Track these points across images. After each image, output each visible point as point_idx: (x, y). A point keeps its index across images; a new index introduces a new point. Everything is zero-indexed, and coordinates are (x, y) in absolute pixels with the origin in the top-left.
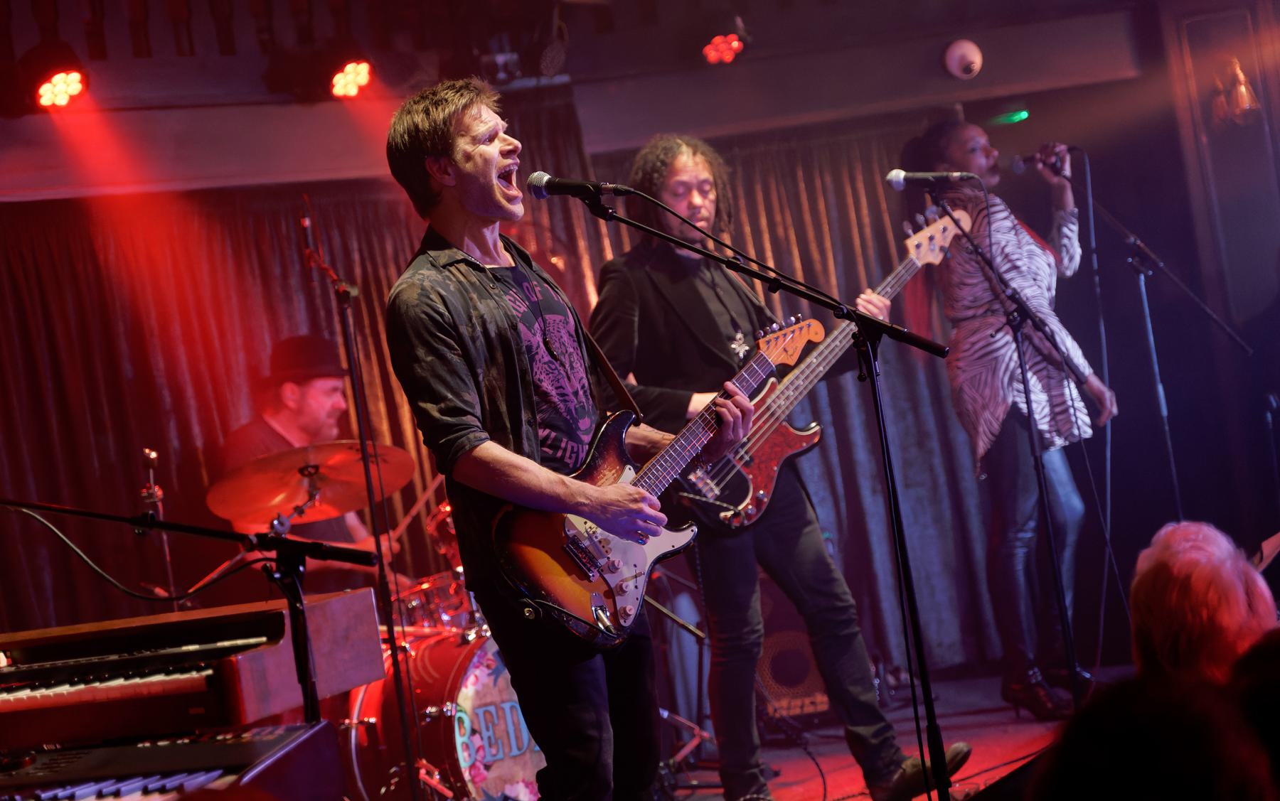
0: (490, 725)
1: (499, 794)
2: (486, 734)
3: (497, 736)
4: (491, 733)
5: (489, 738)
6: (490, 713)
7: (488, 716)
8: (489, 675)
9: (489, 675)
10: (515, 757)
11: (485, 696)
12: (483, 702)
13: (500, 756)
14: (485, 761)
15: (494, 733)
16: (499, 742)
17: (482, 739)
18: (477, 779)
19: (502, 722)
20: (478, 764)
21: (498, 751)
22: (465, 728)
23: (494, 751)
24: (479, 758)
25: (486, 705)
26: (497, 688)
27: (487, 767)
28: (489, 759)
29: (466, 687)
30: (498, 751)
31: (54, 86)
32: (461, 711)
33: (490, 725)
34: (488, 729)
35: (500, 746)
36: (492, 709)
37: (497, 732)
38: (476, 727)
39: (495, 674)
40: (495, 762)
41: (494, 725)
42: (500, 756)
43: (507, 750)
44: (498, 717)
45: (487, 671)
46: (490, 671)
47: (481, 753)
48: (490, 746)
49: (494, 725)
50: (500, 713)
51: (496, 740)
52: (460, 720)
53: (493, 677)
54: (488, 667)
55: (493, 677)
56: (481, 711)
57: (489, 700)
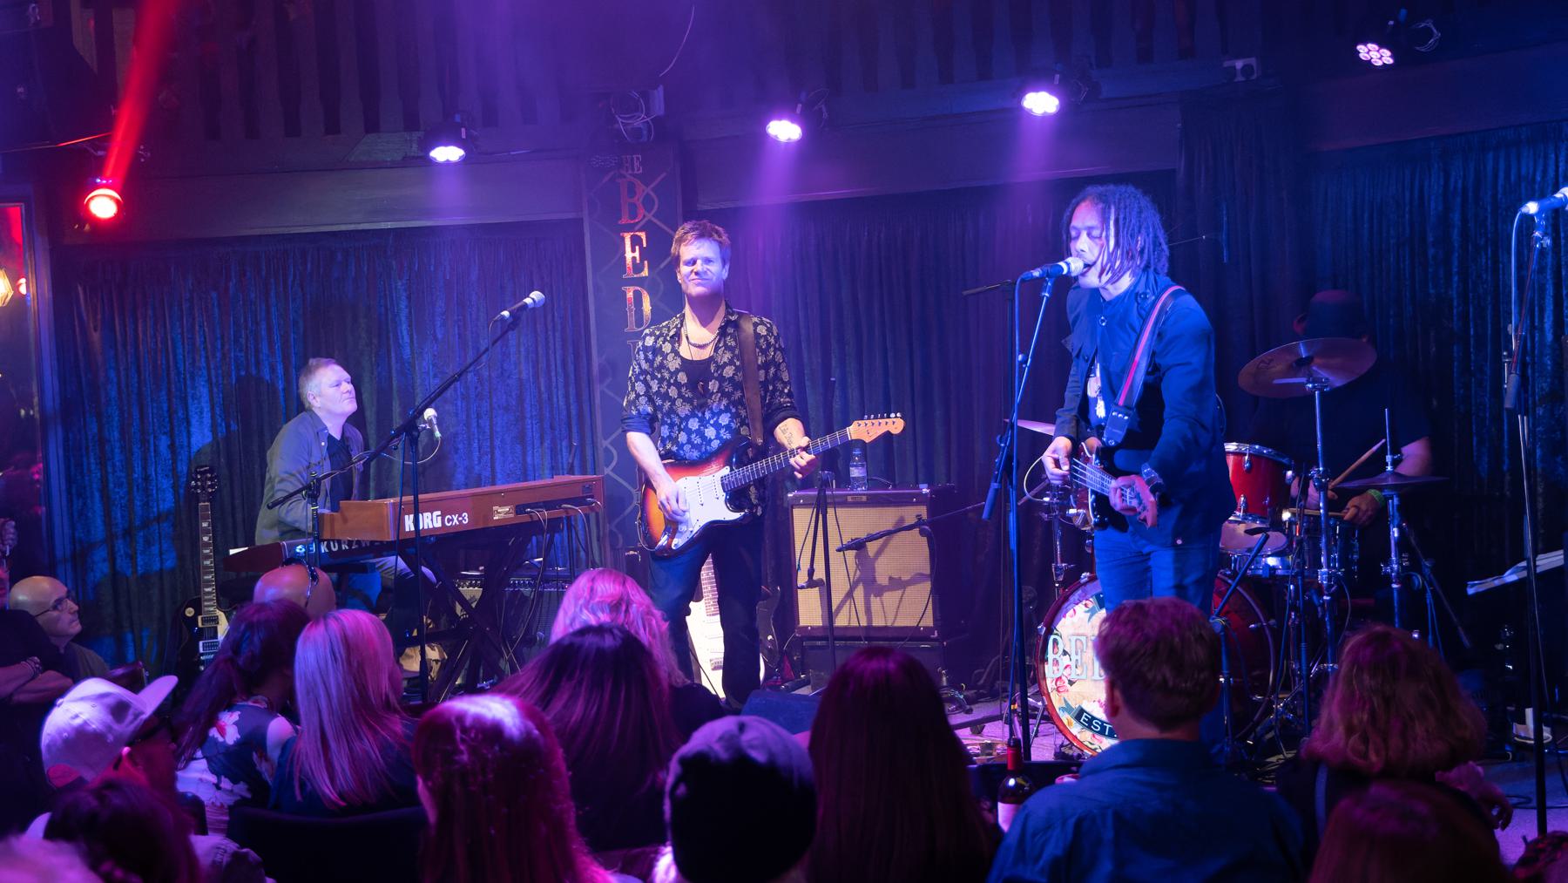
1: (1077, 706)
2: (1074, 657)
3: (1084, 660)
4: (1078, 657)
5: (1077, 660)
6: (1082, 643)
7: (1079, 643)
8: (1086, 612)
9: (1086, 612)
10: (1095, 681)
12: (1077, 632)
13: (1084, 677)
15: (1081, 659)
18: (1061, 690)
20: (1064, 678)
23: (1079, 671)
24: (1066, 674)
25: (1078, 635)
27: (1071, 683)
28: (1069, 678)
32: (1056, 634)
34: (1077, 654)
35: (1085, 669)
36: (1083, 639)
39: (1092, 612)
41: (1082, 651)
42: (1084, 677)
43: (1090, 673)
44: (1087, 646)
45: (1083, 607)
46: (1087, 609)
47: (1068, 669)
49: (1082, 651)
51: (1082, 665)
52: (1055, 642)
53: (1089, 614)
54: (1086, 605)
55: (1089, 614)
57: (1081, 631)
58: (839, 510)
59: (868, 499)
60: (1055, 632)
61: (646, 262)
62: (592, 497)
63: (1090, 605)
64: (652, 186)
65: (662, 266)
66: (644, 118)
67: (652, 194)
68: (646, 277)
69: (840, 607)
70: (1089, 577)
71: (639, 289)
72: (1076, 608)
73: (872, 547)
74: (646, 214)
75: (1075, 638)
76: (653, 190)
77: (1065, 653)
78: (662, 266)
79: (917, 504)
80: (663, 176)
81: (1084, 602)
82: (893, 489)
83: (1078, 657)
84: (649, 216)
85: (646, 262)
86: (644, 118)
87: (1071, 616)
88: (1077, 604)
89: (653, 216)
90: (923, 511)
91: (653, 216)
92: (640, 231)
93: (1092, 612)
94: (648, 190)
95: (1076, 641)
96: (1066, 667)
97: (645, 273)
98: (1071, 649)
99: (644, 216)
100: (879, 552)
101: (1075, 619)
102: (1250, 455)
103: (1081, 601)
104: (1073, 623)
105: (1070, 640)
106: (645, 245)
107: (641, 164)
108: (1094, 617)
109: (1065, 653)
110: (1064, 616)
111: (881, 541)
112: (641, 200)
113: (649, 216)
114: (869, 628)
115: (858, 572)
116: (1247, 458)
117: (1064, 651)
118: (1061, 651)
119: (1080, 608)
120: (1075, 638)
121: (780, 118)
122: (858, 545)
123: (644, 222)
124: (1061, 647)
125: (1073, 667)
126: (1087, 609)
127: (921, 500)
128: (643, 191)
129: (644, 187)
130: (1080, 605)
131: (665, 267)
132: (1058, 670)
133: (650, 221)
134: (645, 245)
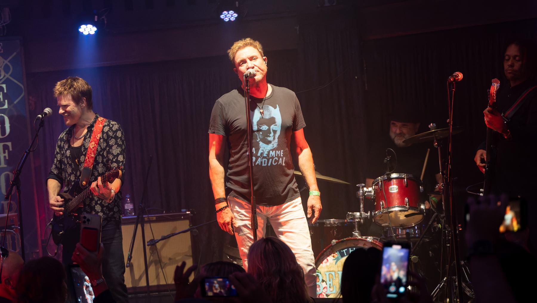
0: (331, 279)
2: (328, 283)
3: (334, 284)
4: (331, 282)
5: (330, 284)
6: (332, 274)
7: (331, 276)
11: (330, 268)
12: (329, 270)
14: (326, 293)
16: (335, 286)
17: (326, 284)
19: (337, 279)
20: (323, 294)
21: (333, 290)
22: (319, 279)
23: (331, 289)
24: (324, 291)
25: (330, 271)
26: (336, 265)
28: (328, 293)
29: (322, 263)
30: (333, 290)
31: (229, 18)
32: (318, 272)
33: (331, 279)
34: (330, 281)
36: (333, 273)
37: (334, 282)
38: (324, 279)
39: (337, 260)
40: (331, 294)
41: (333, 279)
44: (335, 277)
45: (332, 257)
46: (334, 258)
47: (325, 289)
48: (330, 287)
49: (333, 279)
50: (337, 275)
53: (335, 261)
54: (333, 256)
56: (327, 274)
57: (332, 269)
58: (152, 224)
59: (156, 218)
60: (317, 271)
61: (6, 101)
62: (14, 225)
63: (336, 256)
64: (10, 58)
65: (15, 102)
66: (2, 24)
67: (9, 64)
68: (5, 109)
69: (140, 278)
70: (336, 242)
71: (3, 115)
72: (328, 258)
73: (159, 245)
74: (6, 74)
75: (328, 273)
76: (9, 62)
77: (323, 281)
78: (15, 102)
79: (184, 219)
80: (15, 53)
81: (332, 255)
82: (165, 214)
83: (331, 282)
84: (8, 76)
85: (6, 101)
86: (2, 24)
87: (326, 263)
88: (329, 256)
89: (10, 75)
90: (187, 222)
91: (10, 75)
92: (3, 83)
93: (337, 260)
94: (6, 62)
95: (329, 274)
96: (324, 288)
97: (6, 106)
98: (327, 279)
99: (4, 76)
100: (163, 246)
101: (328, 264)
102: (406, 178)
103: (330, 255)
104: (327, 266)
105: (325, 274)
106: (5, 91)
107: (2, 48)
108: (338, 262)
109: (323, 281)
110: (322, 262)
111: (164, 240)
112: (2, 67)
113: (8, 76)
114: (159, 286)
115: (152, 258)
116: (405, 180)
117: (323, 280)
118: (321, 280)
119: (330, 258)
120: (328, 273)
121: (86, 24)
122: (153, 243)
123: (5, 78)
124: (321, 278)
125: (328, 287)
126: (334, 258)
127: (186, 217)
128: (4, 62)
129: (5, 61)
130: (330, 256)
131: (18, 103)
132: (320, 290)
133: (8, 79)
134: (5, 91)
